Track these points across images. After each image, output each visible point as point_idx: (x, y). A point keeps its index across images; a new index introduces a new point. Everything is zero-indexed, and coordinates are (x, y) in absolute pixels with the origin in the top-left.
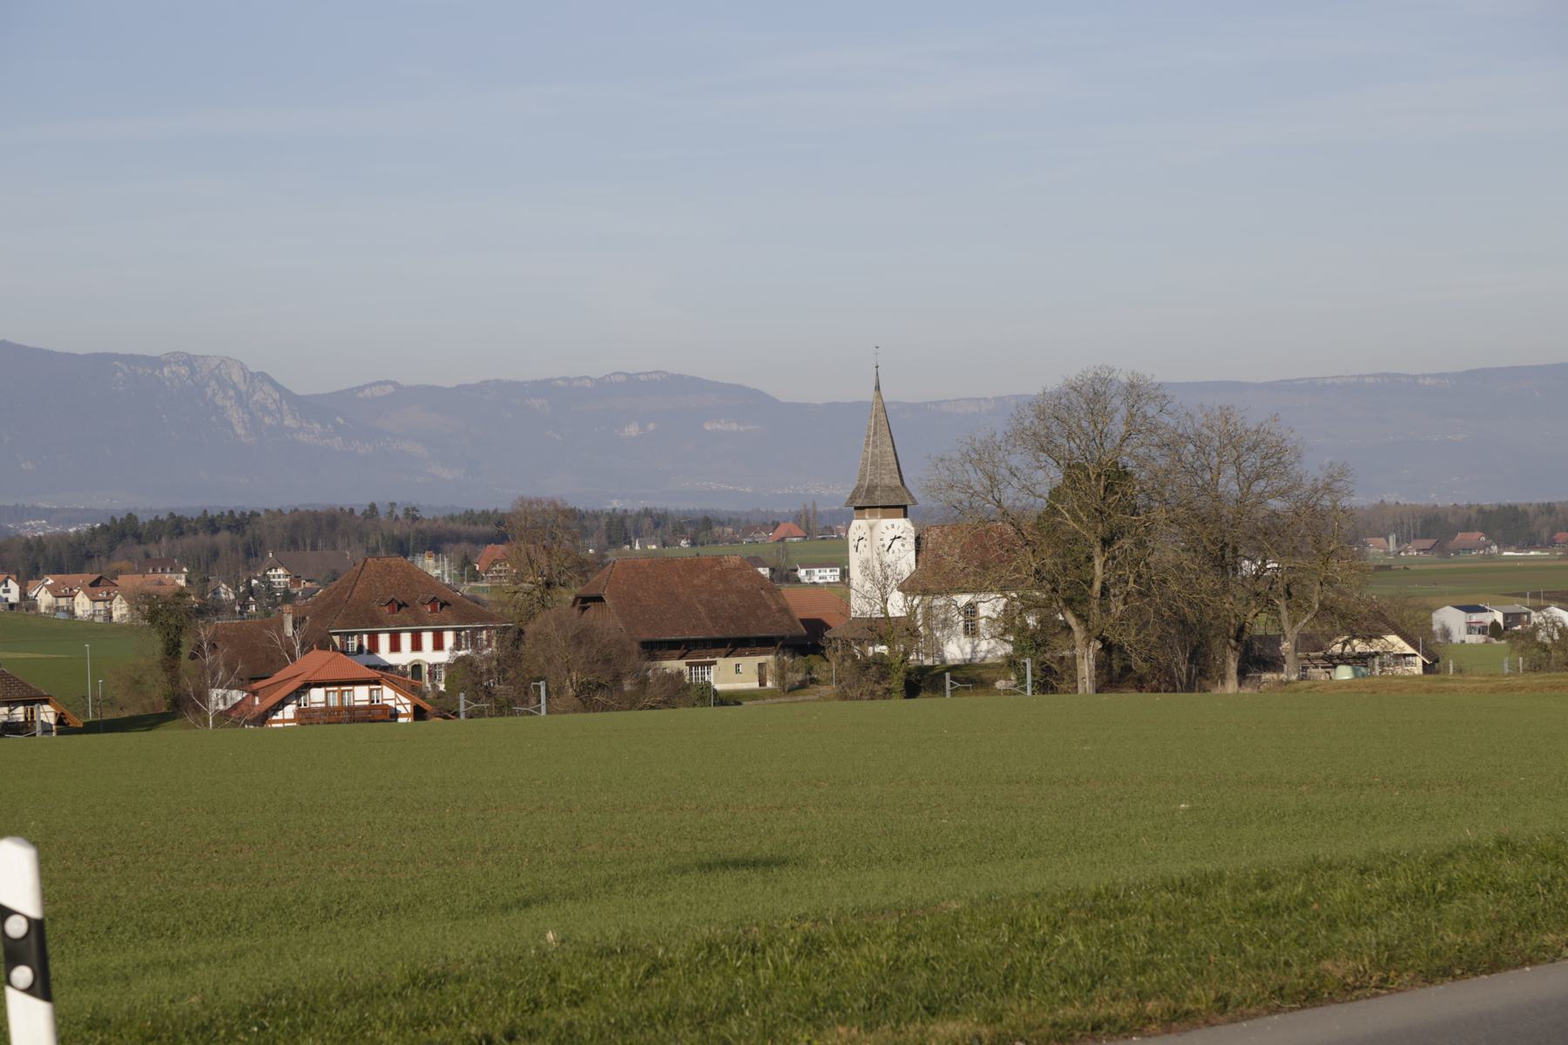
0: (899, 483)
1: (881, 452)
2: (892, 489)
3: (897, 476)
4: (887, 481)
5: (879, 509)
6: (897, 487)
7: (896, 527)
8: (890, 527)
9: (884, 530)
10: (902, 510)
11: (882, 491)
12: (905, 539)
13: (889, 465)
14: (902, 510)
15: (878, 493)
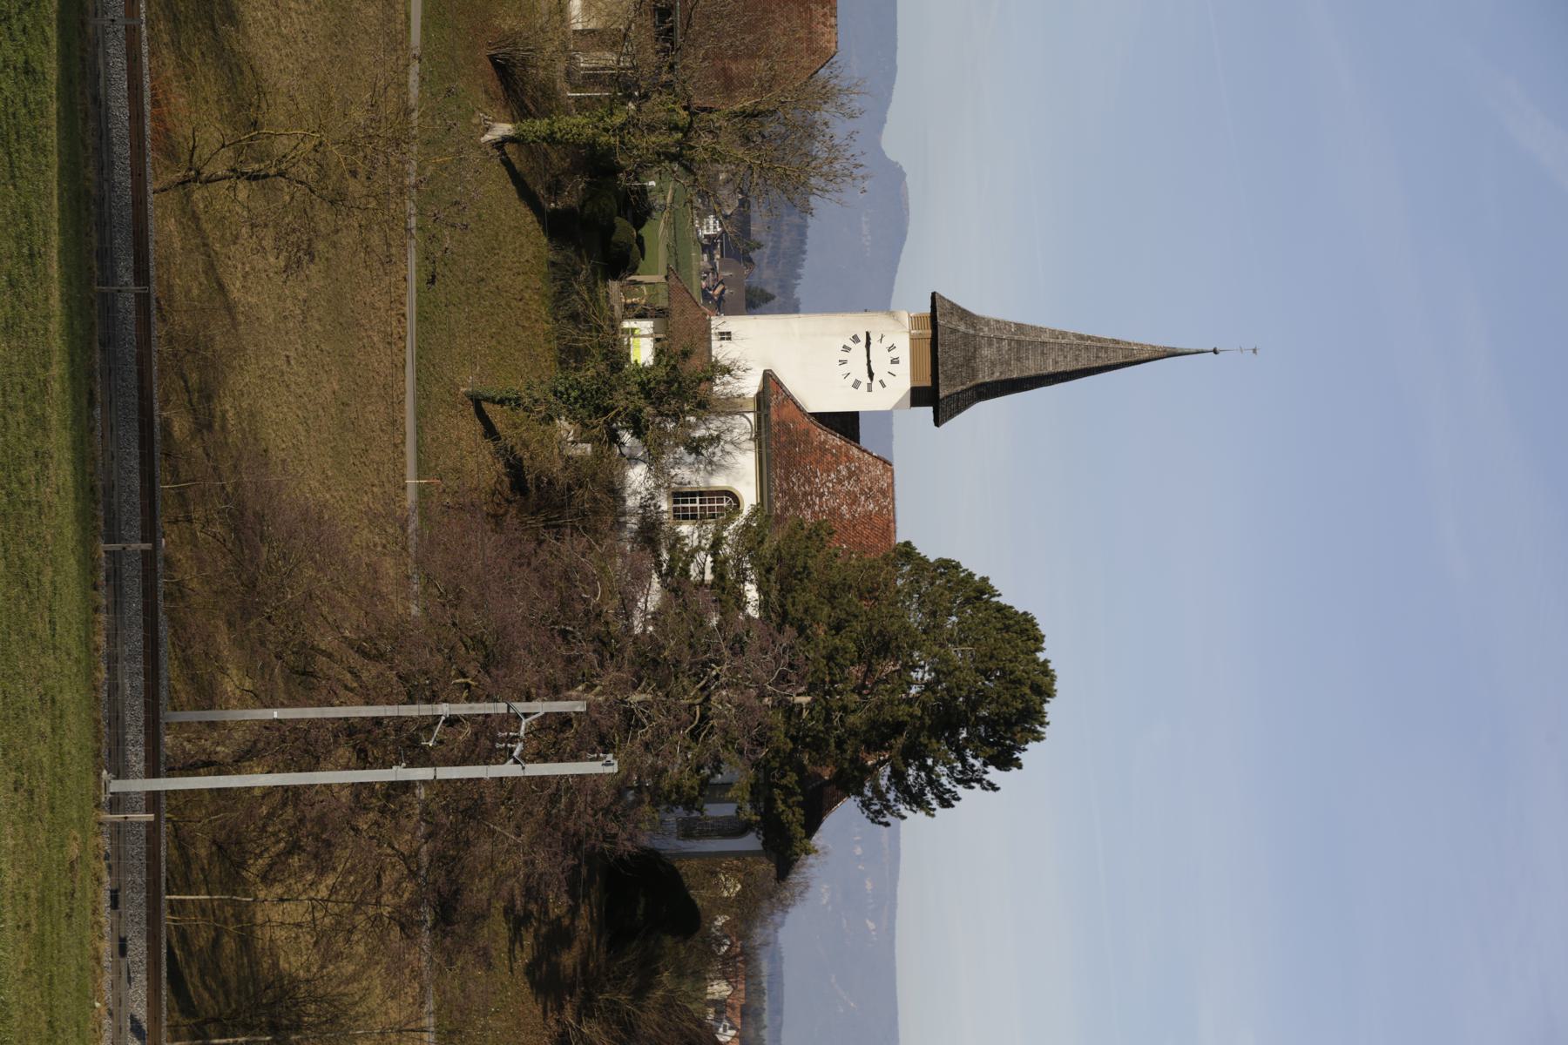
0: (984, 377)
1: (1043, 343)
2: (969, 360)
3: (996, 376)
4: (986, 352)
5: (929, 332)
6: (973, 373)
7: (894, 368)
8: (894, 354)
9: (887, 342)
10: (927, 383)
11: (966, 335)
12: (870, 390)
13: (1019, 359)
14: (927, 383)
15: (962, 328)
